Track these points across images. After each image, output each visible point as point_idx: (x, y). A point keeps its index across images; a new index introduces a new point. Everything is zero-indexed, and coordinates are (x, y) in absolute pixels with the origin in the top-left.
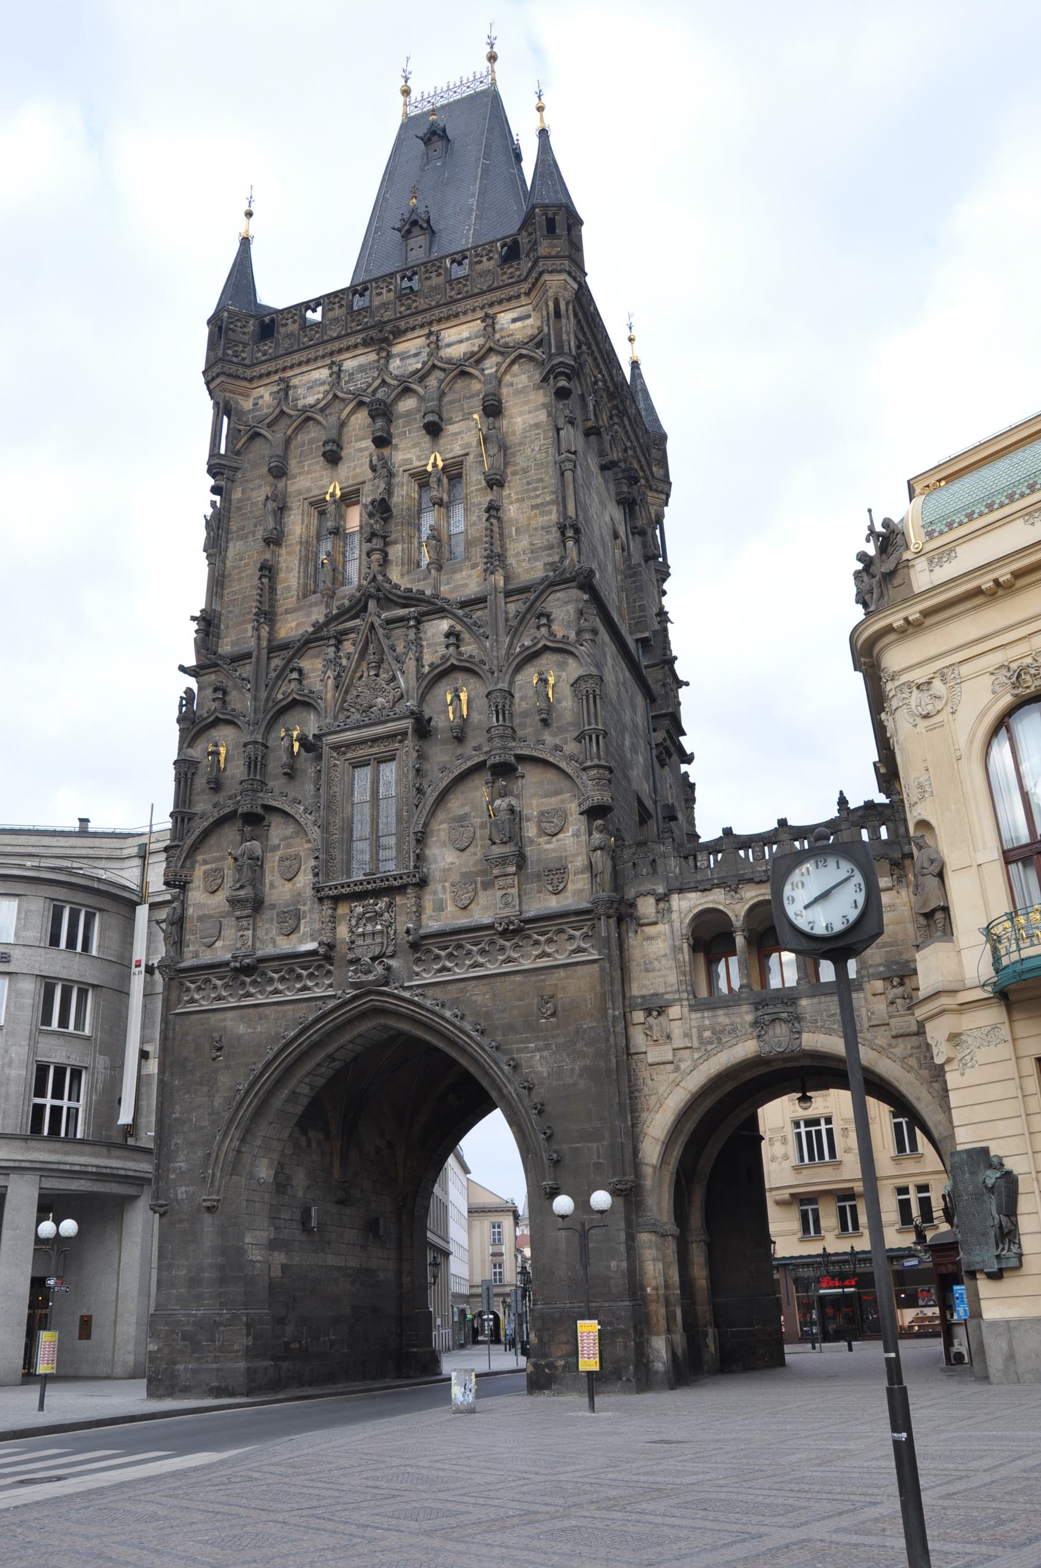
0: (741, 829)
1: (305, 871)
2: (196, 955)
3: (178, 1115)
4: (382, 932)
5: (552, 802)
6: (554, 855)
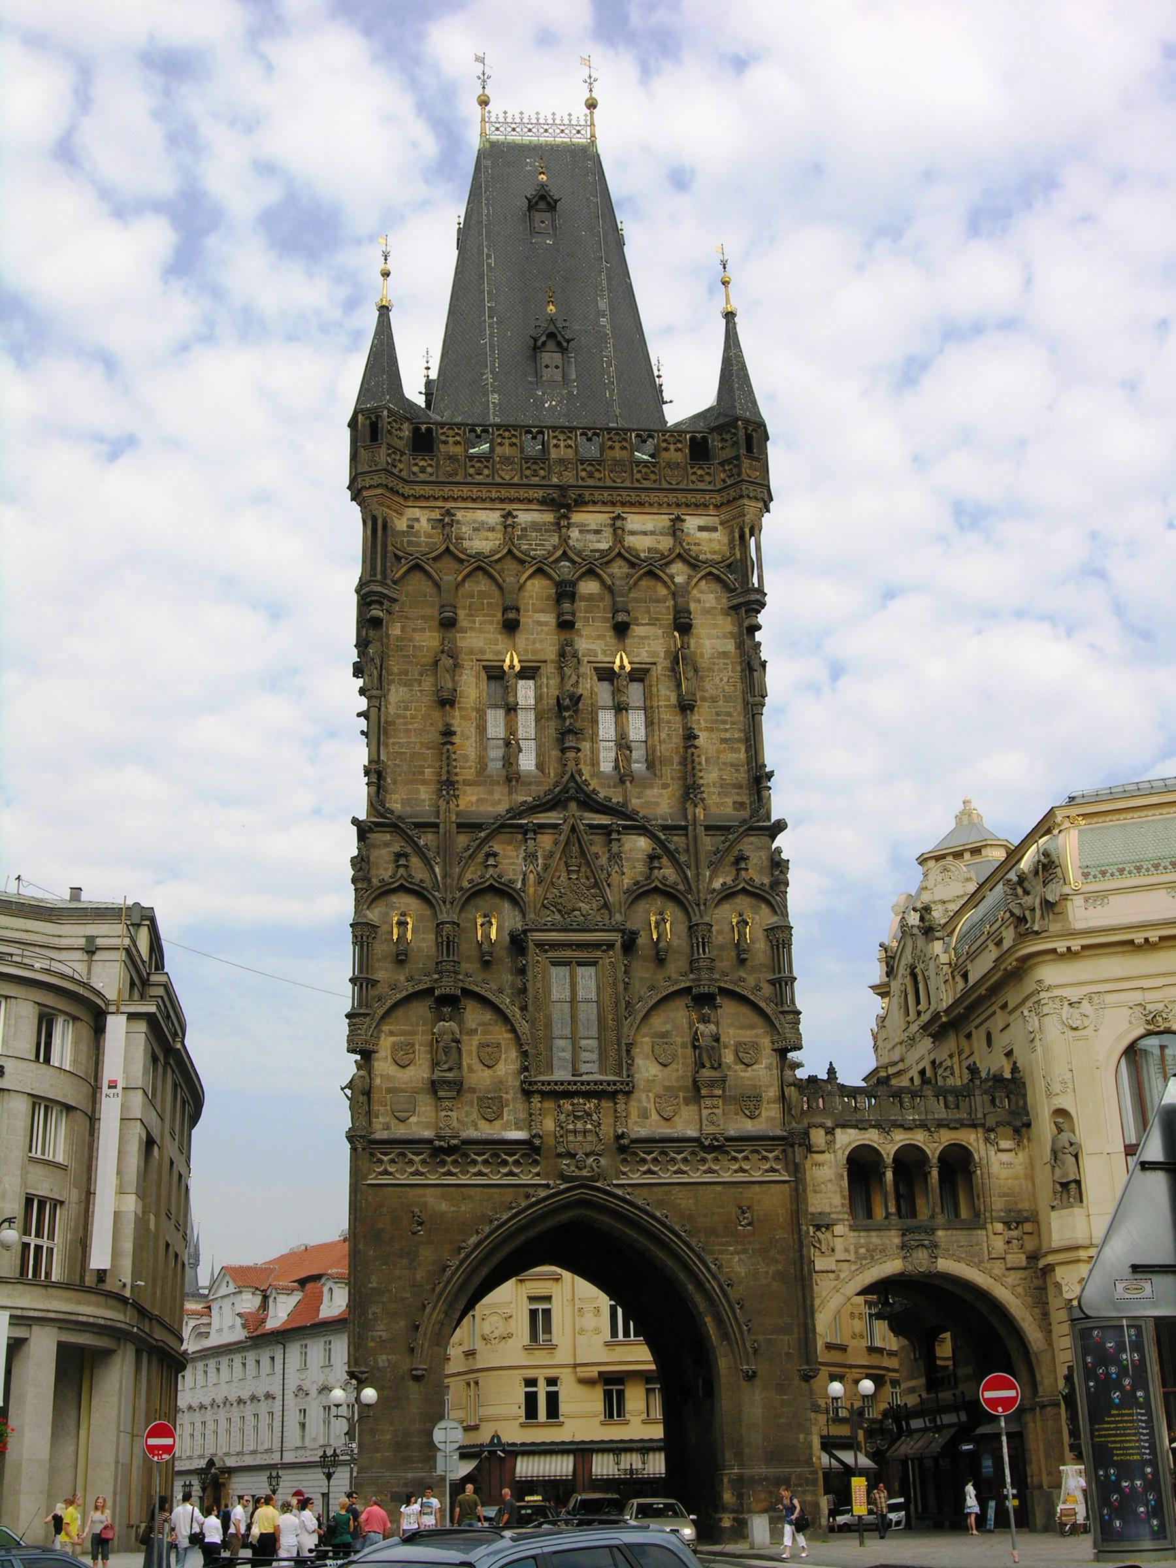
1: (506, 1060)
2: (387, 1127)
3: (375, 1285)
4: (591, 1131)
6: (750, 1083)
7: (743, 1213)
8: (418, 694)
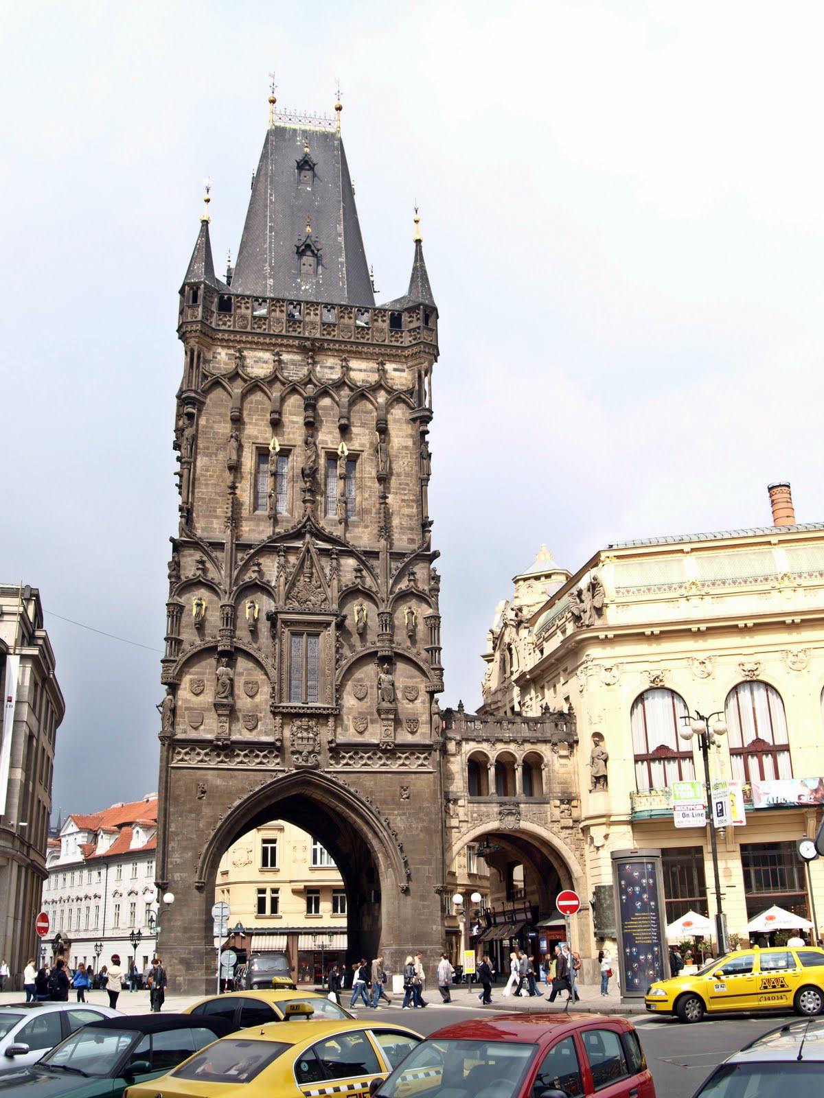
6: (410, 711)
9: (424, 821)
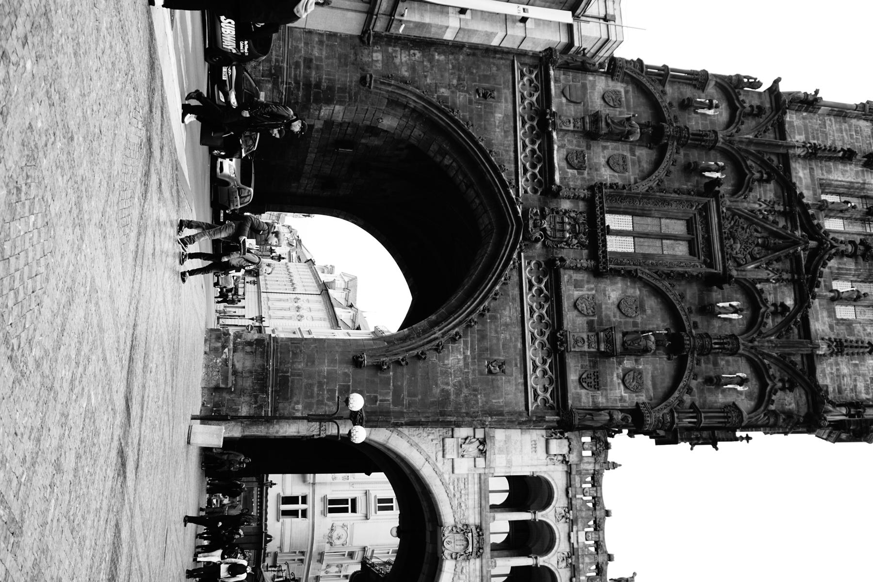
0: (609, 524)
1: (613, 176)
3: (437, 57)
4: (564, 237)
5: (649, 384)
6: (609, 380)
7: (499, 367)
8: (868, 142)
9: (458, 394)
